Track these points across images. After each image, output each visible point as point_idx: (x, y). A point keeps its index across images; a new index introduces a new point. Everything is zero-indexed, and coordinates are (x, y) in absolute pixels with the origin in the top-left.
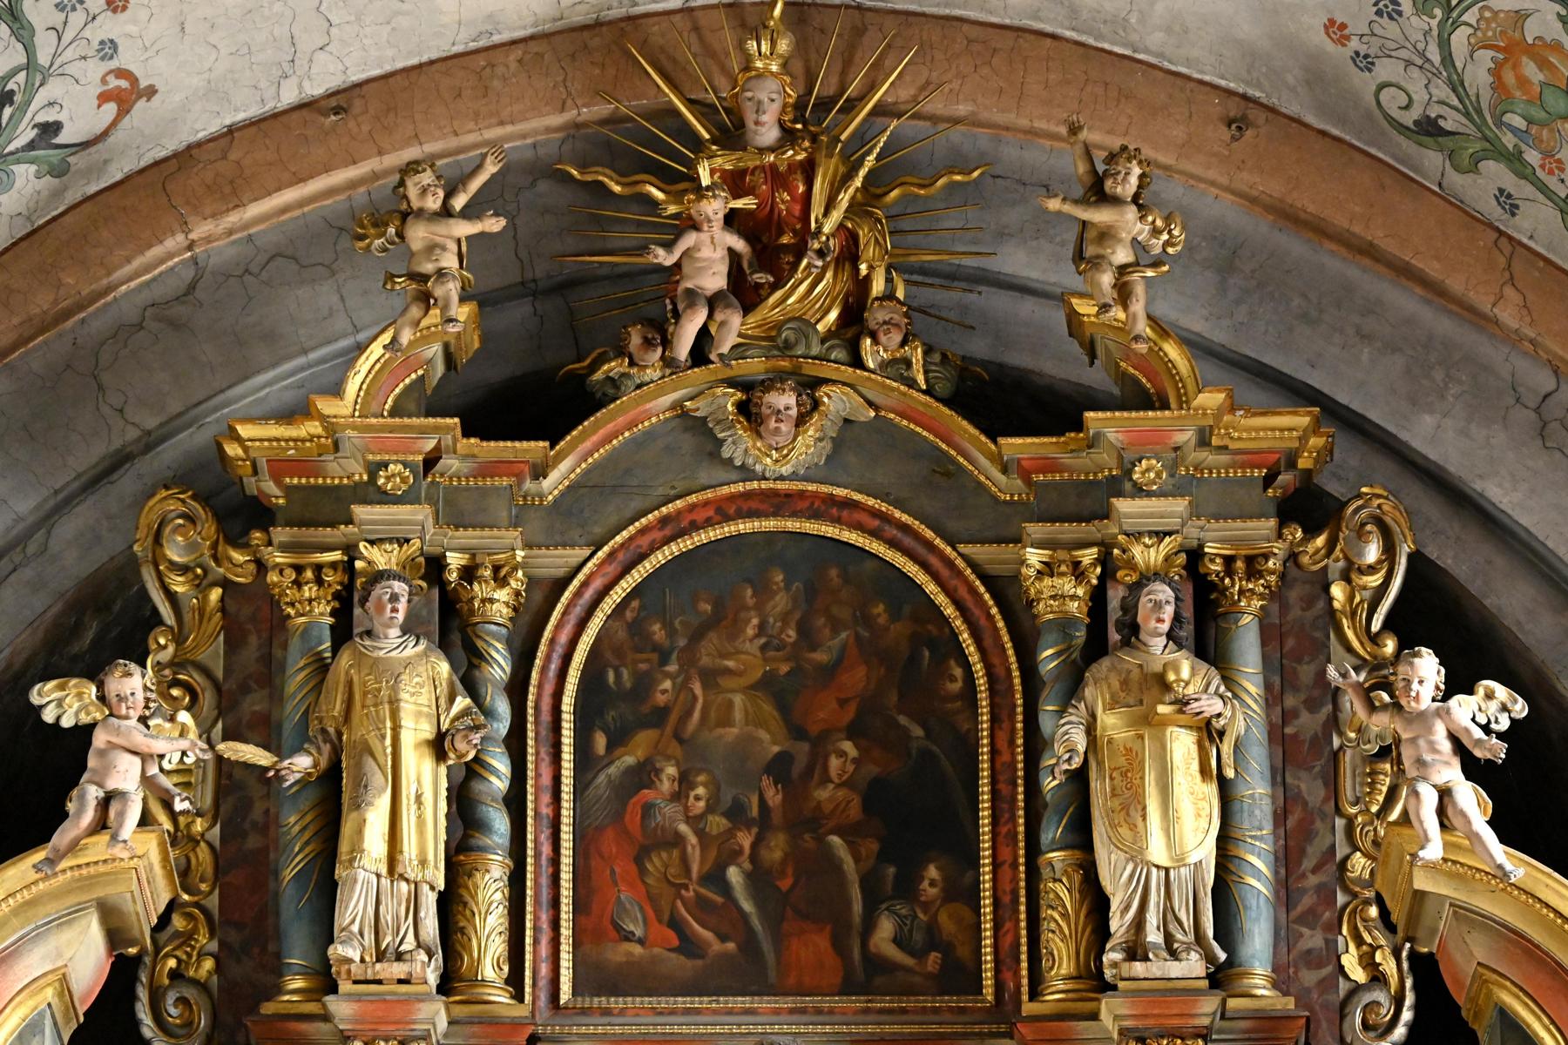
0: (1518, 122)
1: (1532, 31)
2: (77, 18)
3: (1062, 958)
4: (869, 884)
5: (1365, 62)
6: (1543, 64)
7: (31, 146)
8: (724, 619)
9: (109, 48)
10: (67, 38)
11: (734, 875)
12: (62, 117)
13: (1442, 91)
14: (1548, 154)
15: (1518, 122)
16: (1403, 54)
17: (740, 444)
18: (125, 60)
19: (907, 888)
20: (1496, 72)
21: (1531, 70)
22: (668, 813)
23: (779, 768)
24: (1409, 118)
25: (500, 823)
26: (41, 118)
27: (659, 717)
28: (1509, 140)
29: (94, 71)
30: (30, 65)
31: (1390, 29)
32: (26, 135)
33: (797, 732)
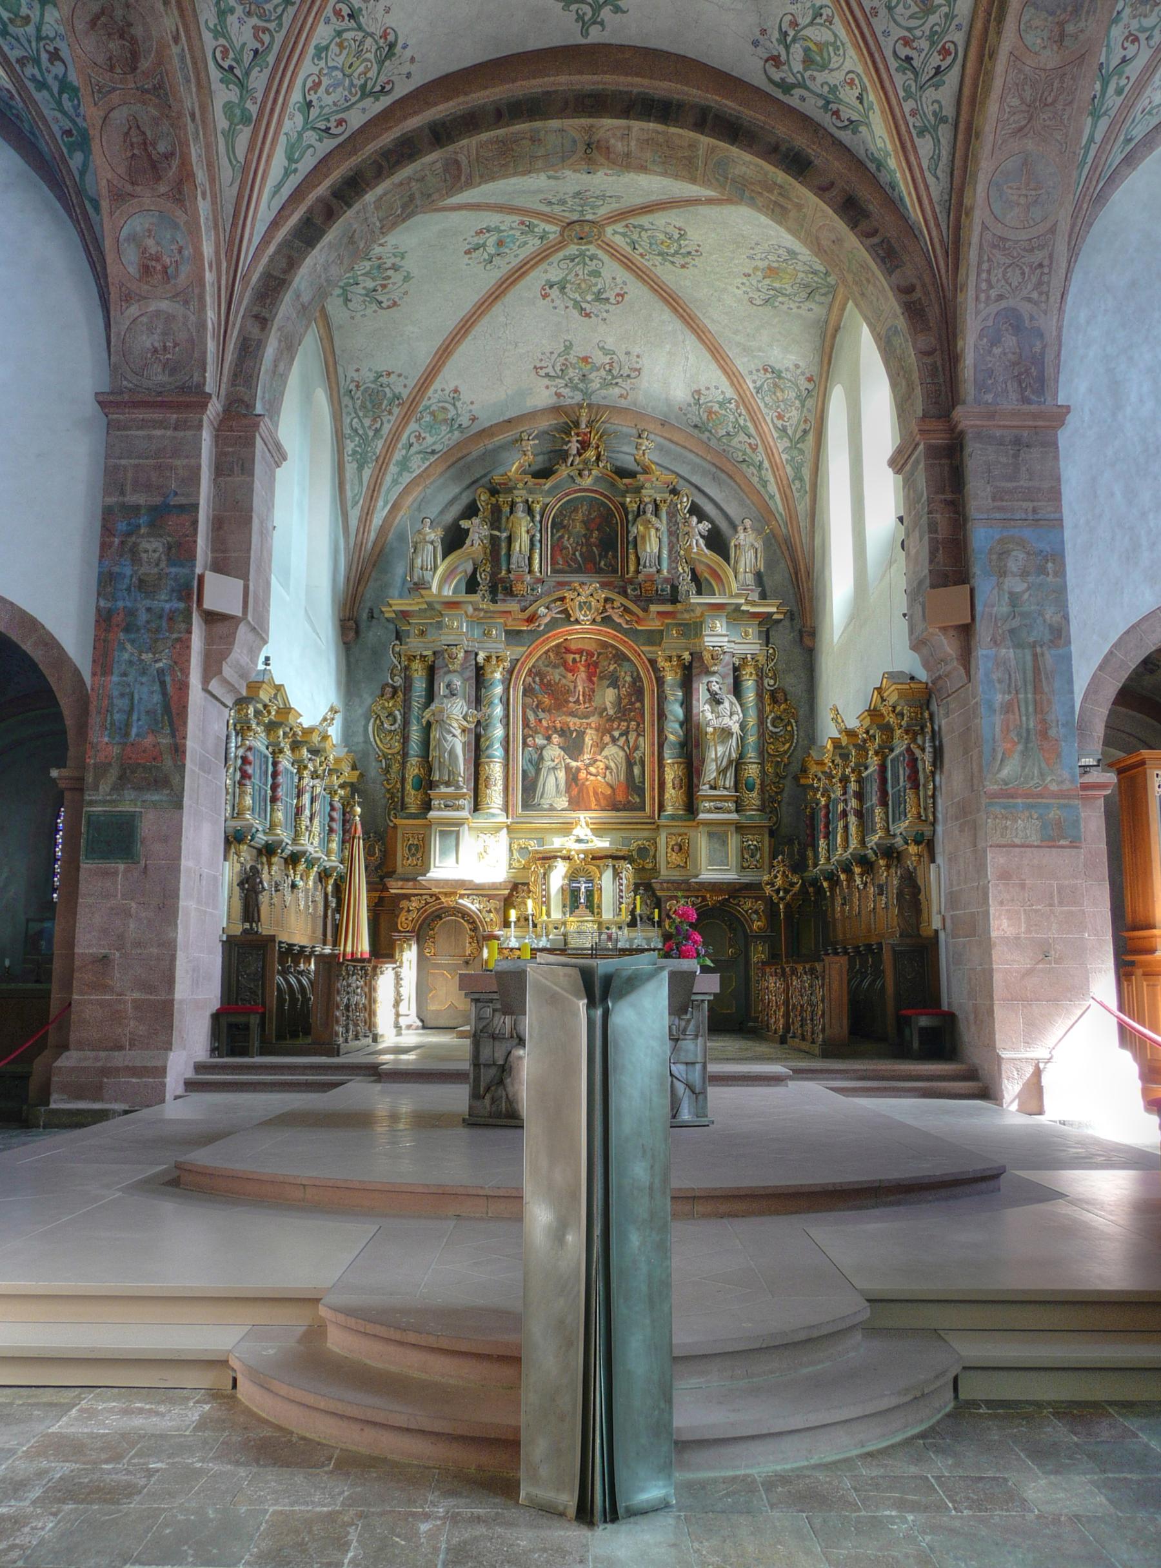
3: (632, 568)
4: (600, 555)
8: (576, 510)
11: (577, 554)
17: (578, 480)
19: (606, 556)
22: (566, 543)
23: (585, 536)
25: (538, 545)
27: (564, 527)
33: (587, 529)
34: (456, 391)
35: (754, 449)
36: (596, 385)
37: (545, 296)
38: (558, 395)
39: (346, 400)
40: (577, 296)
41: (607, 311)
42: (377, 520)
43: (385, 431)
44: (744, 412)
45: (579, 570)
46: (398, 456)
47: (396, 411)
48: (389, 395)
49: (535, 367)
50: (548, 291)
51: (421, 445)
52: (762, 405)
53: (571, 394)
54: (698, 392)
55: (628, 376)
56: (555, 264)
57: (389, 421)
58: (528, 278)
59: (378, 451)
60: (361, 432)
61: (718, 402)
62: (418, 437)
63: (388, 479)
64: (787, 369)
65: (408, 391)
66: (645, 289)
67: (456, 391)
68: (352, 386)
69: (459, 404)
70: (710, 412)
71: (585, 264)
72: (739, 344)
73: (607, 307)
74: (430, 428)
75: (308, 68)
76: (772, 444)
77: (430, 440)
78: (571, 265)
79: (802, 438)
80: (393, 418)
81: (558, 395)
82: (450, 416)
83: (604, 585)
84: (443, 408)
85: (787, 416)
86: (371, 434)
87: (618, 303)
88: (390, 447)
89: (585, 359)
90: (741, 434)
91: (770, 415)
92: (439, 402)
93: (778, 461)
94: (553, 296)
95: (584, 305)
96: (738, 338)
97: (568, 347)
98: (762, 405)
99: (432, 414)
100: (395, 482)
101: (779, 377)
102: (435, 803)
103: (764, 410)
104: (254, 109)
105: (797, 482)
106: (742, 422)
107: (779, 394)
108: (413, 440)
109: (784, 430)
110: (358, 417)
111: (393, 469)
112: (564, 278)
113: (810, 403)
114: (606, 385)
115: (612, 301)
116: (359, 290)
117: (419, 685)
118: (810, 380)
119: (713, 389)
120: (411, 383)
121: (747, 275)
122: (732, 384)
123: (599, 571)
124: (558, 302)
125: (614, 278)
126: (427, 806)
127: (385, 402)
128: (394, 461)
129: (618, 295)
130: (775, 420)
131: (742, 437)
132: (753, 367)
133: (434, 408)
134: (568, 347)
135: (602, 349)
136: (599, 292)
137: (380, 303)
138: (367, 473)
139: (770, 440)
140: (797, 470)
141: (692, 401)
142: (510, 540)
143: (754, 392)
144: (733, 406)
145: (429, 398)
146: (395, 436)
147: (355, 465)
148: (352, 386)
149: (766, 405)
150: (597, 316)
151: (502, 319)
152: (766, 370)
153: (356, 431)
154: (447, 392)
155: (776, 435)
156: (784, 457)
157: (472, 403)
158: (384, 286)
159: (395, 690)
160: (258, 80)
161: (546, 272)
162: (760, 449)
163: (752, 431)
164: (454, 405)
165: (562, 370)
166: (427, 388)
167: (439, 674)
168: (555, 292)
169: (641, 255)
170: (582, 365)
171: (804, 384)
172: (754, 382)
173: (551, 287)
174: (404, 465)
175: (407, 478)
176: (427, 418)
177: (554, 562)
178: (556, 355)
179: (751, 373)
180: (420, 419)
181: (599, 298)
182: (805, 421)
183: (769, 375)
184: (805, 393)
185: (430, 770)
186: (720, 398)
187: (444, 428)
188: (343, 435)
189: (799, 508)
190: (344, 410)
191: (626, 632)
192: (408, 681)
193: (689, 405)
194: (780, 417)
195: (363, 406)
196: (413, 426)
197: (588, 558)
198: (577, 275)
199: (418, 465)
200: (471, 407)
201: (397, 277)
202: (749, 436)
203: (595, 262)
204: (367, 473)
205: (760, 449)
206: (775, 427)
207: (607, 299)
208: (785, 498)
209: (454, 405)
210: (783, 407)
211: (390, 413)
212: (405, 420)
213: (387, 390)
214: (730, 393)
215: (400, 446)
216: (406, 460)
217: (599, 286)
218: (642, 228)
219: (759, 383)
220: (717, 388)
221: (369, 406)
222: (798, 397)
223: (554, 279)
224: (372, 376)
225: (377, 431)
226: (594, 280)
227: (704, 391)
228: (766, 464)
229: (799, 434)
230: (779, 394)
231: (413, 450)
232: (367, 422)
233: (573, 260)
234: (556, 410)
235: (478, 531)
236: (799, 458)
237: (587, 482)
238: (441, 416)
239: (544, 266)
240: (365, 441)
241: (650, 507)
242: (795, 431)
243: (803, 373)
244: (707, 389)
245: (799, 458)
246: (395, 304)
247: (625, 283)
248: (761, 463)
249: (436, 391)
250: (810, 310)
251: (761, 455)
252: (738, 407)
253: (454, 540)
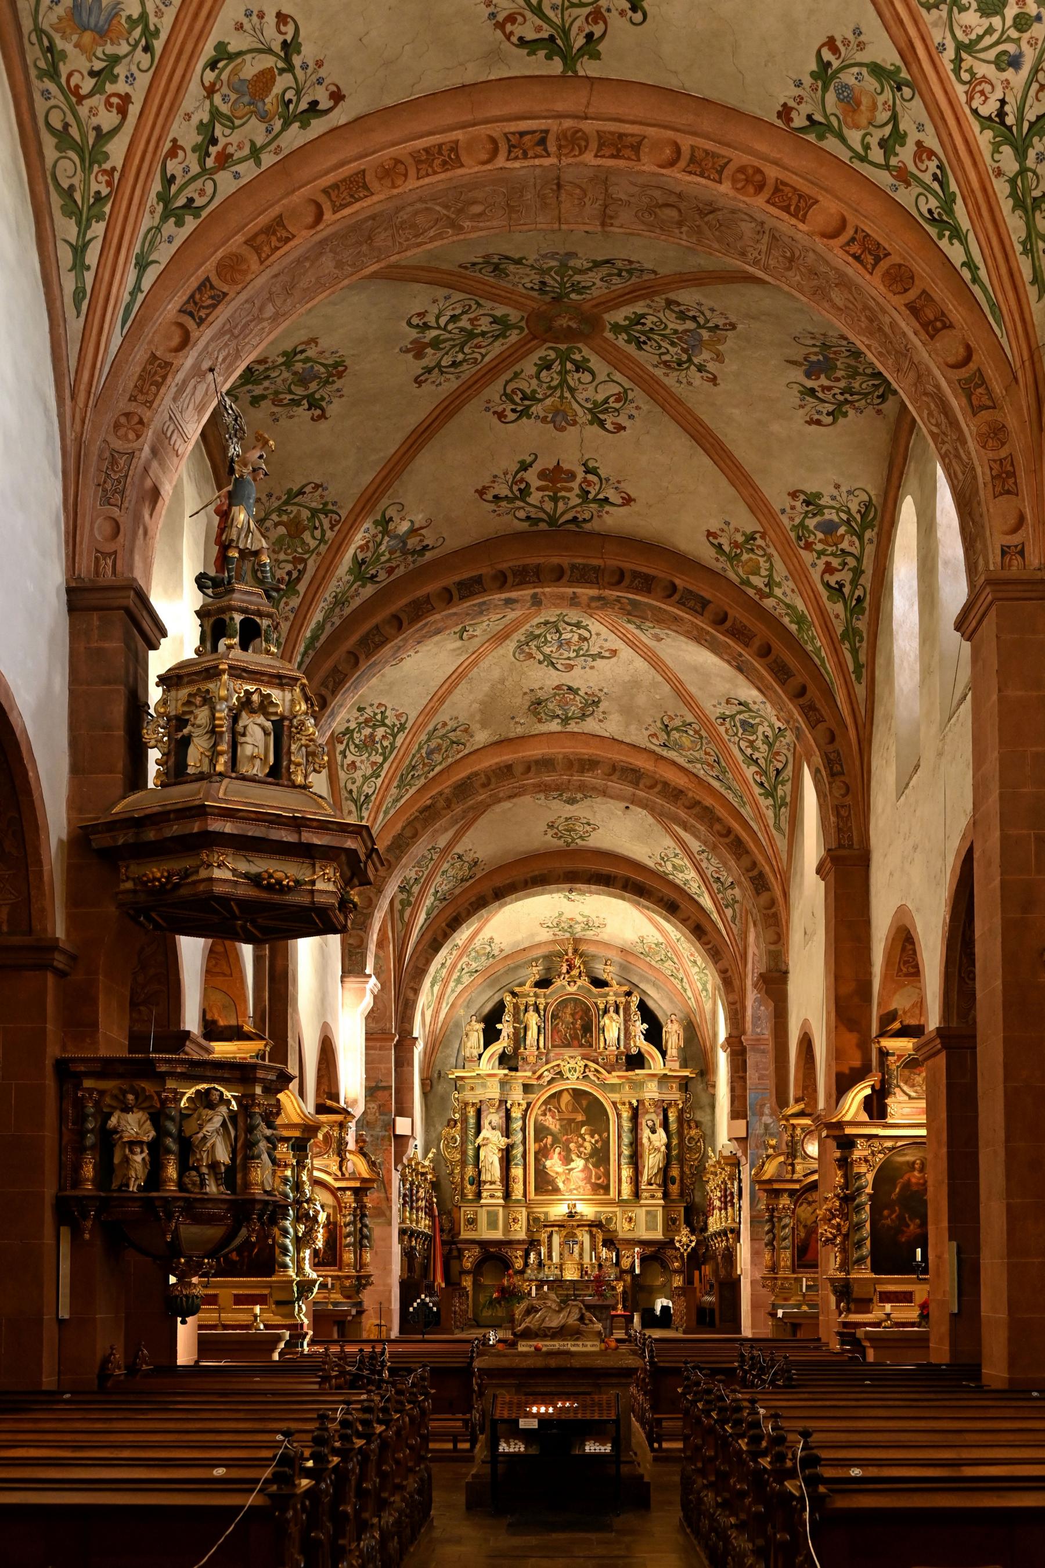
3: (602, 1045)
42: (442, 1016)
45: (568, 1045)
46: (455, 976)
62: (468, 965)
63: (449, 990)
74: (475, 959)
75: (438, 879)
77: (474, 965)
83: (584, 1057)
88: (450, 973)
97: (561, 914)
100: (453, 991)
102: (485, 1194)
104: (413, 900)
111: (452, 984)
114: (584, 930)
117: (472, 1121)
123: (581, 1046)
126: (479, 1195)
140: (704, 985)
142: (526, 1029)
146: (454, 966)
159: (456, 1122)
160: (416, 889)
167: (484, 1115)
174: (458, 981)
175: (460, 987)
176: (473, 954)
177: (553, 1040)
185: (480, 1172)
191: (597, 1085)
192: (465, 1120)
196: (465, 959)
197: (574, 1037)
199: (466, 980)
204: (436, 988)
208: (697, 1001)
212: (460, 956)
214: (661, 940)
216: (459, 977)
234: (555, 942)
235: (506, 1028)
237: (572, 989)
241: (612, 1009)
251: (681, 975)
253: (491, 1036)
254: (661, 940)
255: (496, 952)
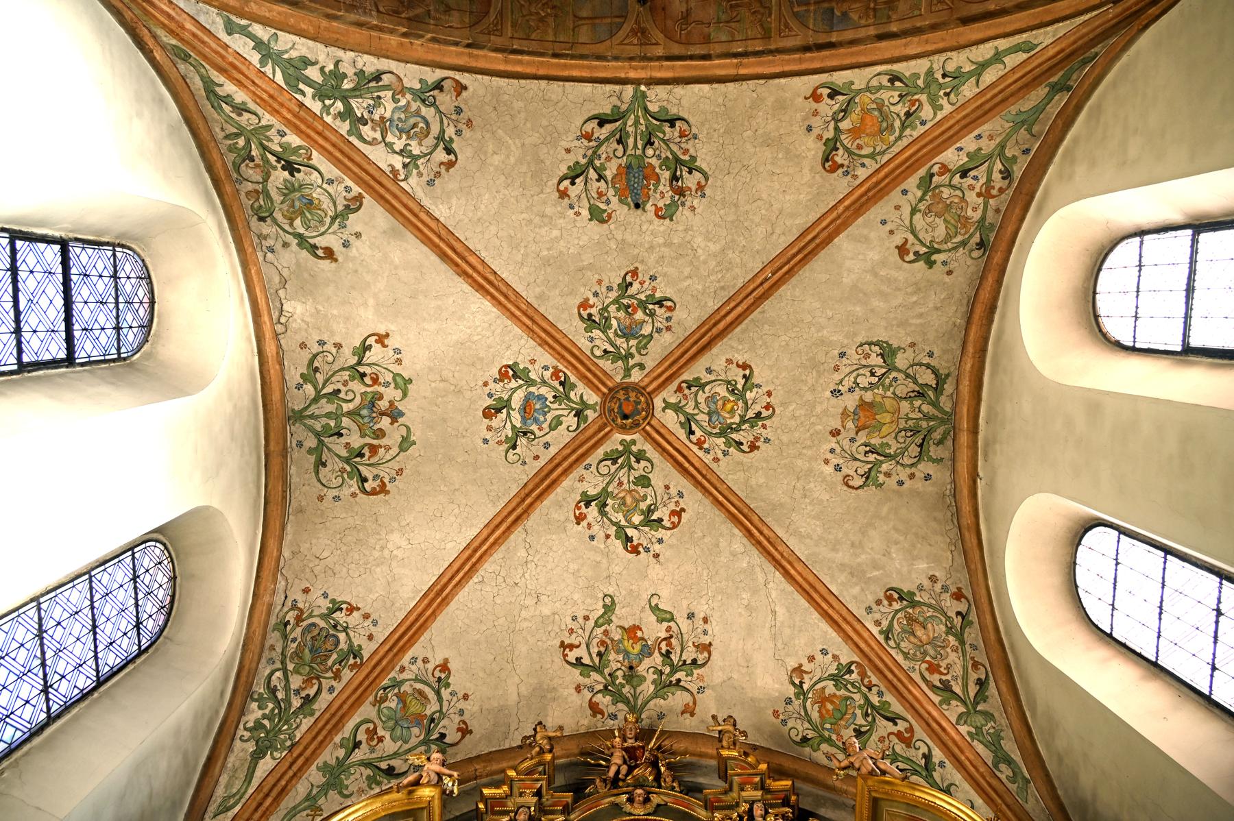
0: (828, 726)
1: (827, 692)
2: (455, 699)
5: (784, 722)
6: (832, 703)
7: (437, 739)
9: (461, 712)
10: (452, 704)
12: (447, 733)
13: (807, 725)
14: (838, 734)
15: (828, 726)
16: (795, 716)
18: (466, 717)
20: (820, 712)
21: (830, 707)
24: (798, 739)
26: (441, 731)
28: (826, 734)
29: (457, 719)
30: (440, 711)
31: (790, 708)
32: (435, 736)
34: (444, 667)
35: (907, 739)
36: (648, 688)
37: (579, 519)
38: (595, 708)
39: (274, 638)
40: (620, 518)
41: (660, 541)
43: (320, 705)
44: (874, 680)
46: (331, 754)
47: (347, 674)
48: (343, 646)
49: (563, 645)
50: (584, 510)
51: (372, 750)
52: (900, 658)
53: (612, 709)
54: (799, 670)
55: (694, 661)
56: (593, 469)
57: (331, 689)
58: (559, 490)
59: (298, 736)
60: (280, 695)
61: (832, 677)
62: (372, 733)
64: (921, 588)
65: (373, 646)
66: (707, 502)
67: (444, 667)
68: (291, 616)
69: (445, 693)
70: (822, 700)
71: (631, 468)
72: (842, 567)
73: (661, 533)
76: (935, 713)
77: (389, 746)
78: (613, 468)
79: (981, 696)
80: (339, 686)
81: (595, 708)
82: (428, 712)
84: (420, 692)
85: (943, 664)
86: (296, 703)
87: (674, 526)
89: (632, 632)
90: (882, 723)
91: (917, 670)
92: (416, 680)
93: (957, 738)
94: (590, 518)
95: (630, 532)
96: (839, 557)
98: (900, 658)
99: (401, 698)
101: (914, 604)
103: (905, 664)
105: (1003, 767)
106: (875, 700)
107: (920, 632)
108: (362, 736)
109: (946, 688)
110: (284, 670)
112: (605, 489)
113: (972, 635)
114: (665, 686)
115: (666, 523)
116: (339, 448)
118: (958, 596)
119: (819, 657)
120: (381, 634)
121: (835, 433)
122: (847, 638)
124: (596, 528)
125: (667, 487)
127: (335, 656)
128: (320, 761)
129: (673, 513)
130: (927, 675)
131: (884, 727)
132: (870, 599)
133: (406, 688)
134: (609, 608)
135: (655, 609)
136: (650, 511)
137: (365, 480)
138: (266, 764)
139: (930, 708)
140: (995, 744)
141: (791, 691)
143: (881, 638)
144: (855, 676)
145: (403, 669)
146: (336, 719)
147: (251, 746)
148: (291, 616)
149: (906, 656)
150: (647, 550)
151: (522, 553)
152: (890, 599)
153: (273, 691)
154: (430, 666)
155: (936, 699)
156: (963, 729)
157: (466, 697)
158: (374, 449)
161: (581, 480)
162: (919, 732)
163: (897, 707)
164: (438, 693)
165: (600, 654)
166: (403, 650)
168: (592, 512)
169: (699, 444)
170: (628, 644)
171: (952, 607)
172: (878, 623)
173: (588, 505)
176: (393, 703)
178: (591, 623)
179: (869, 610)
180: (384, 699)
181: (651, 522)
182: (976, 665)
183: (896, 606)
184: (958, 621)
186: (833, 670)
187: (416, 731)
188: (249, 695)
189: (1029, 807)
190: (266, 654)
193: (788, 701)
194: (933, 669)
195: (298, 654)
198: (620, 484)
200: (462, 705)
201: (394, 437)
202: (893, 720)
203: (643, 463)
205: (919, 732)
206: (933, 687)
207: (660, 520)
209: (438, 693)
210: (932, 652)
211: (337, 676)
213: (342, 636)
214: (847, 655)
215: (337, 739)
217: (648, 502)
218: (698, 384)
219: (885, 624)
220: (824, 652)
221: (307, 655)
222: (950, 630)
223: (593, 492)
224: (325, 604)
225: (308, 700)
226: (642, 491)
227: (807, 667)
228: (938, 755)
229: (973, 690)
230: (920, 632)
231: (358, 755)
232: (296, 682)
233: (615, 461)
236: (989, 727)
238: (414, 707)
239: (579, 471)
240: (283, 712)
242: (965, 687)
243: (945, 589)
244: (811, 659)
245: (989, 727)
246: (383, 489)
247: (681, 495)
248: (927, 757)
249: (414, 660)
250: (928, 477)
252: (863, 675)
254: (847, 655)
255: (449, 728)
